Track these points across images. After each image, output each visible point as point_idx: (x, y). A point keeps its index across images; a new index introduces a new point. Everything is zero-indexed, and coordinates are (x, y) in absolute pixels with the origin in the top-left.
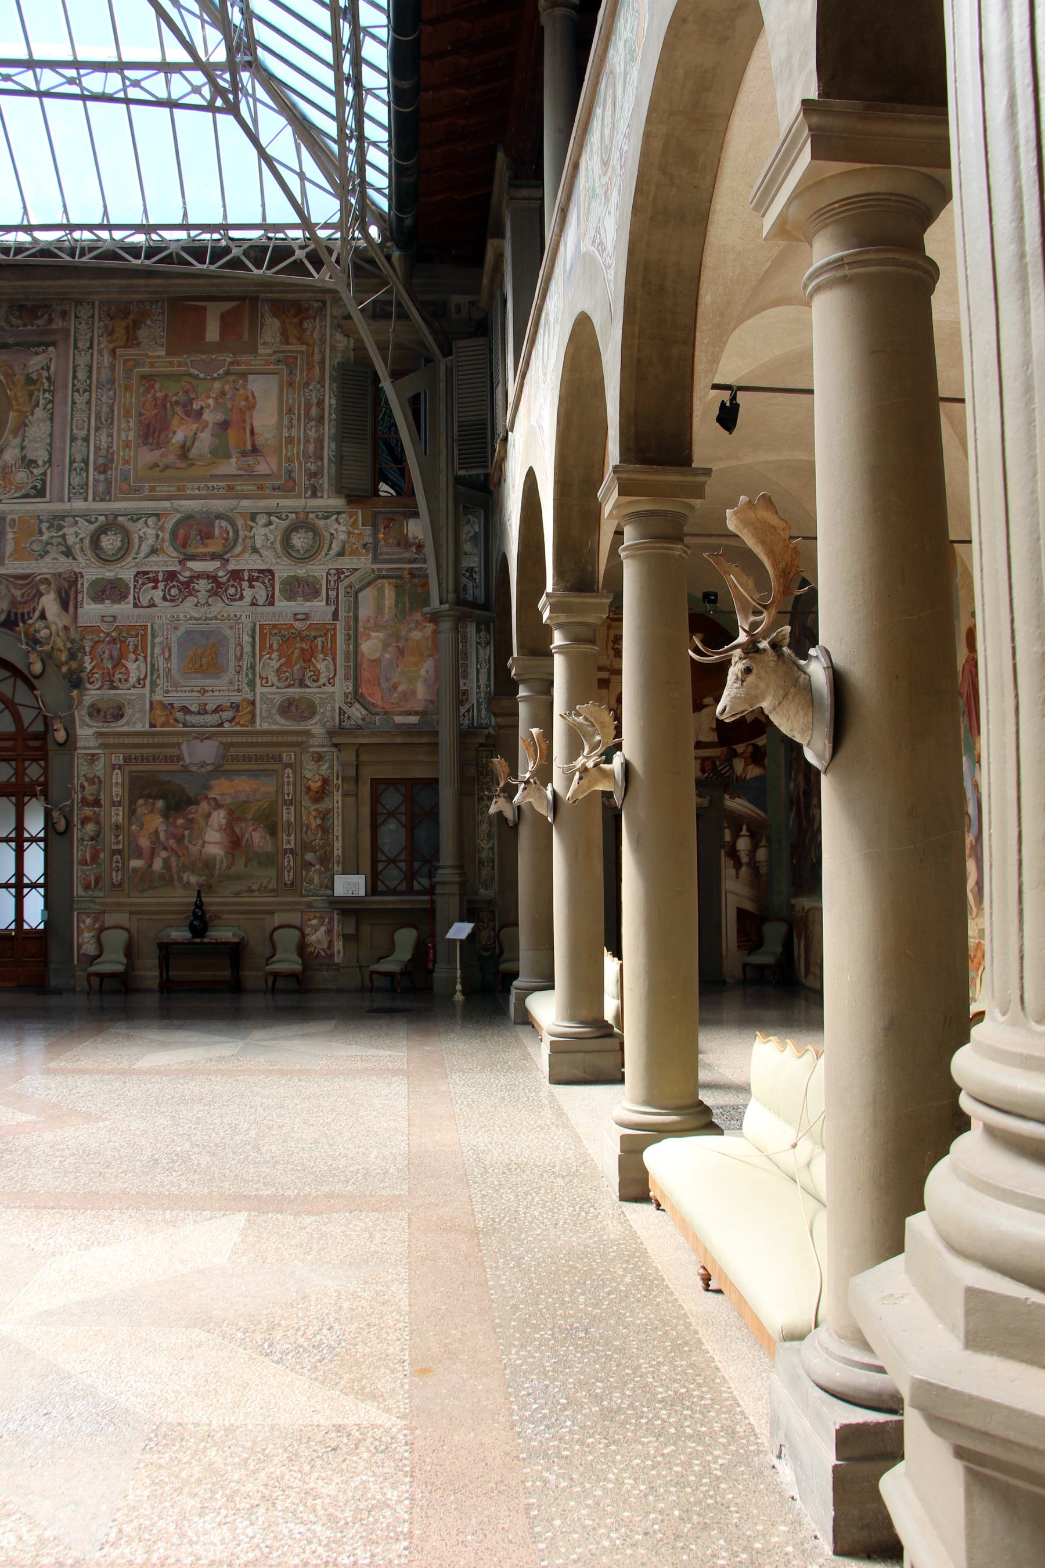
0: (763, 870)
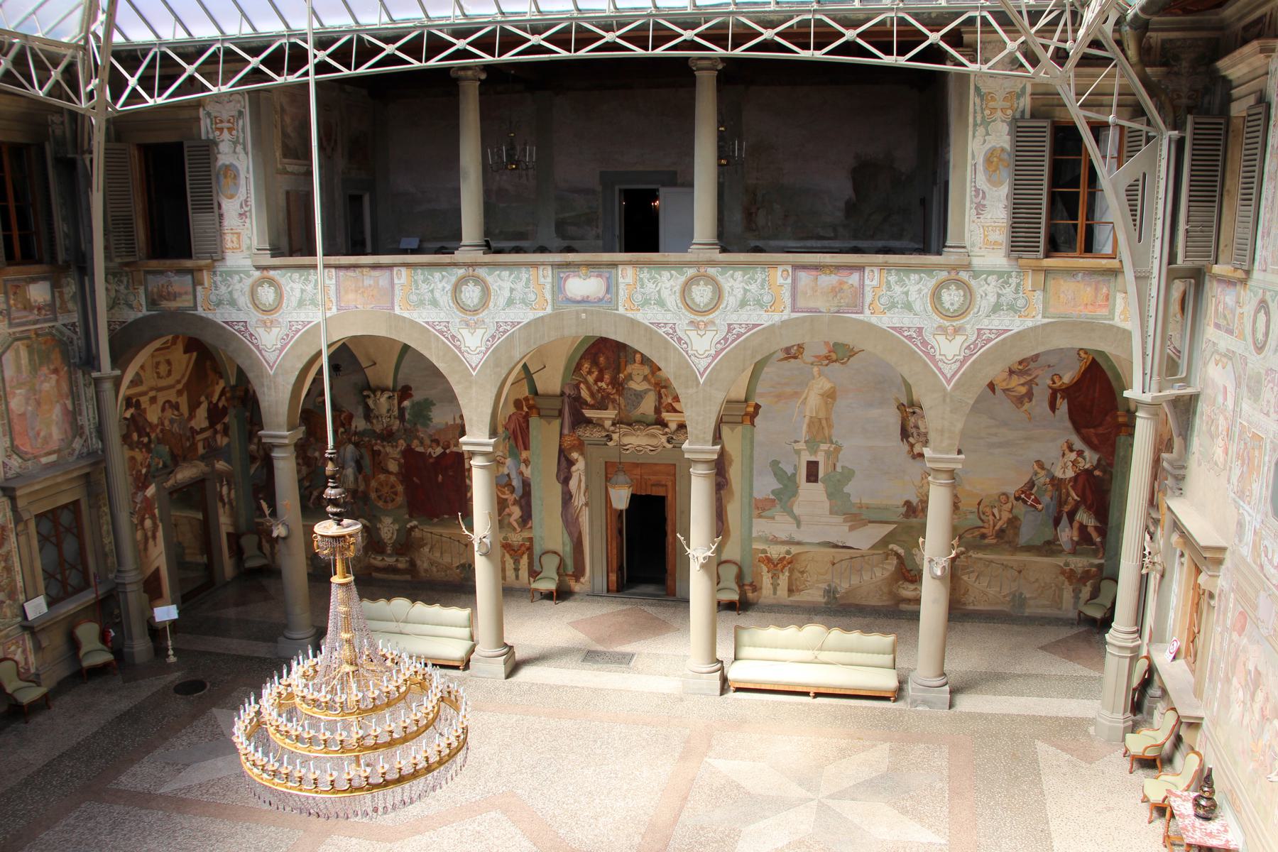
0: (234, 504)
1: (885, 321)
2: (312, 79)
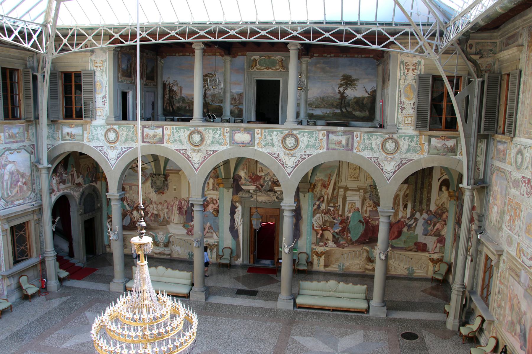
2: (138, 44)
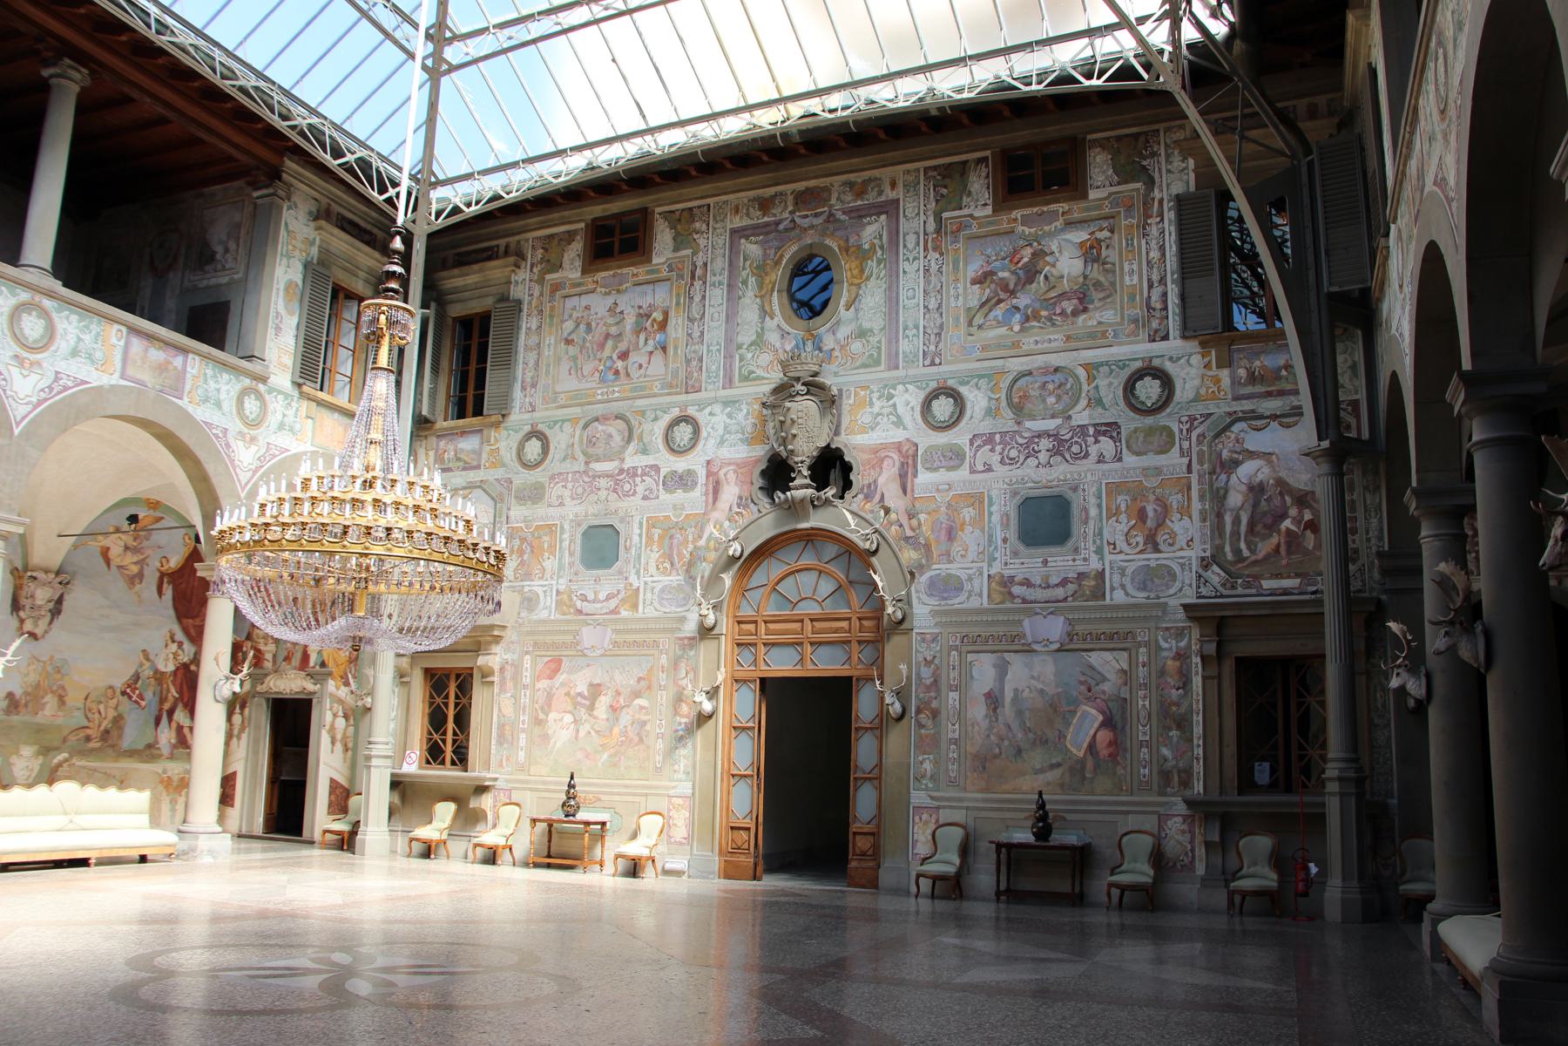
1: (201, 413)
